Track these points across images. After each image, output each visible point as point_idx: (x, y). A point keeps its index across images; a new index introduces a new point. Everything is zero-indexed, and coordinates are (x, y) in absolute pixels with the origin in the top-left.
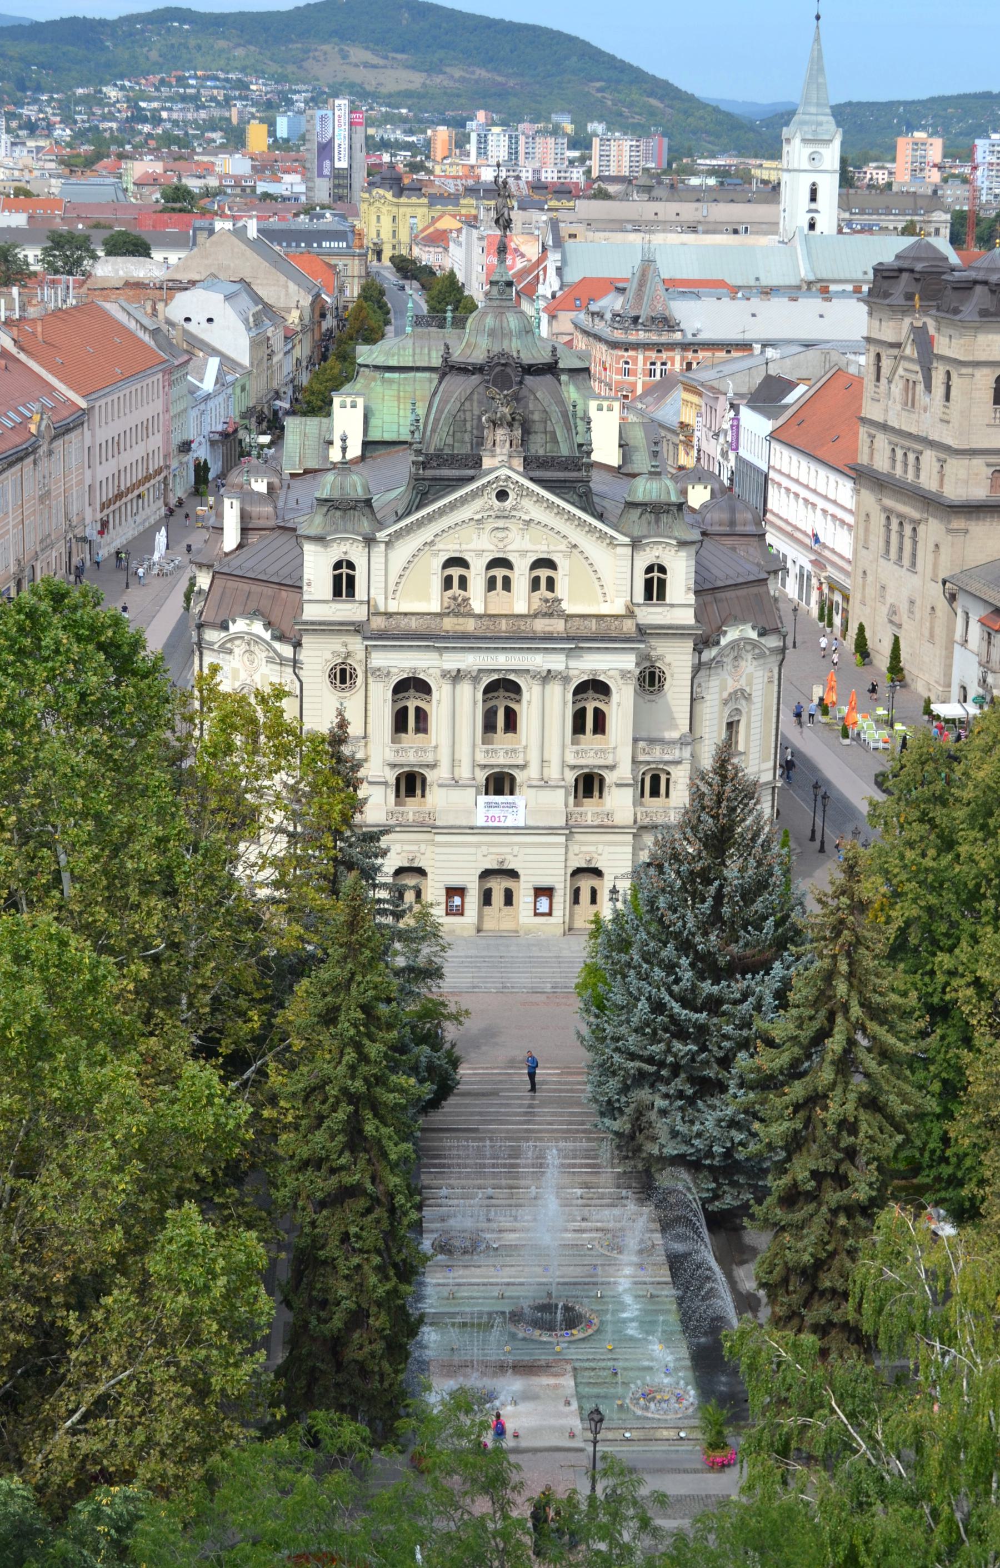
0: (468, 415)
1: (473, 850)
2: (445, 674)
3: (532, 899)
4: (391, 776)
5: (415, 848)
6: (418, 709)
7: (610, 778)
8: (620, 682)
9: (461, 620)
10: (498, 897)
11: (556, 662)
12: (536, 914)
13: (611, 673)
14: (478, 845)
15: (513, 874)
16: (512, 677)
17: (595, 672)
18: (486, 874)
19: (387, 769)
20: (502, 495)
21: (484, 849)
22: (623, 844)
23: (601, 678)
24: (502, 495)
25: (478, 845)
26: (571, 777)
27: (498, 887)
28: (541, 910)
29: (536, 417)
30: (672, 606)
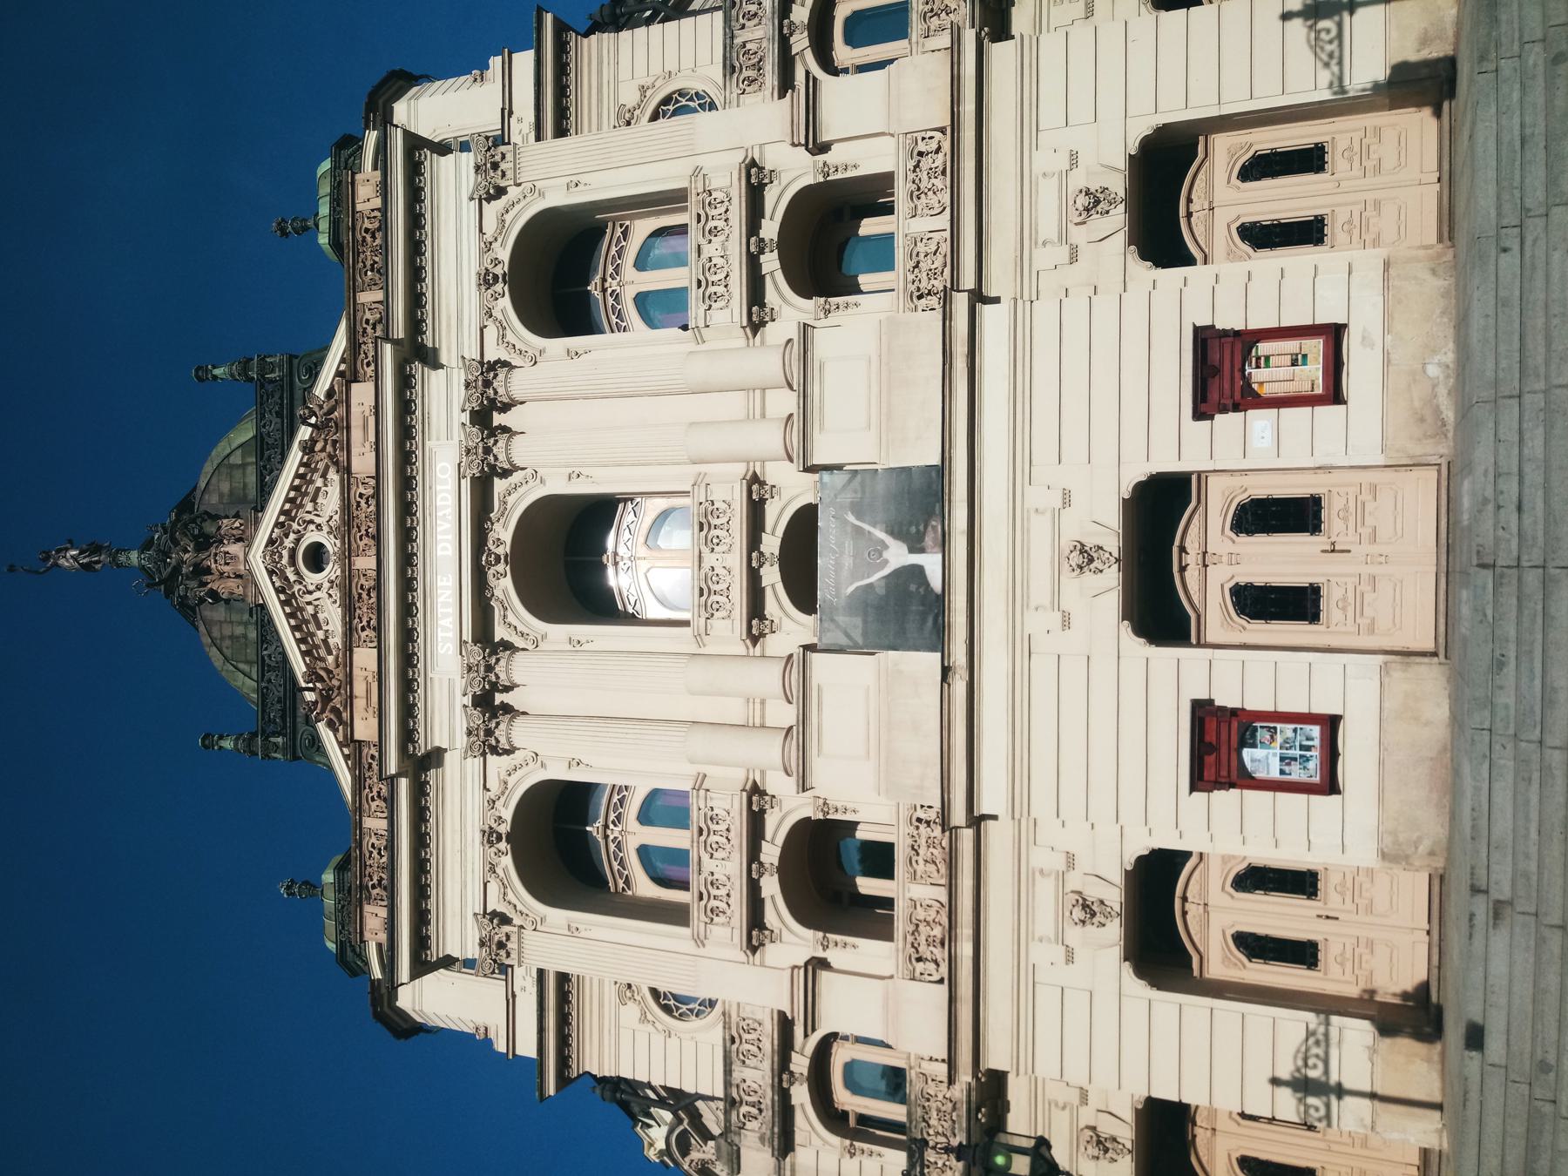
0: (227, 631)
1: (1043, 667)
2: (488, 745)
3: (1260, 420)
4: (794, 942)
5: (1045, 891)
6: (645, 817)
7: (795, 172)
8: (513, 192)
9: (359, 688)
10: (1278, 559)
11: (444, 398)
12: (1334, 394)
13: (490, 226)
14: (1022, 648)
15: (1159, 505)
16: (503, 533)
17: (487, 280)
18: (1158, 613)
19: (771, 952)
20: (316, 557)
21: (1039, 623)
22: (1028, 73)
23: (504, 253)
24: (316, 557)
25: (1022, 648)
26: (790, 309)
27: (1216, 560)
28: (1313, 375)
29: (225, 487)
30: (507, 112)
